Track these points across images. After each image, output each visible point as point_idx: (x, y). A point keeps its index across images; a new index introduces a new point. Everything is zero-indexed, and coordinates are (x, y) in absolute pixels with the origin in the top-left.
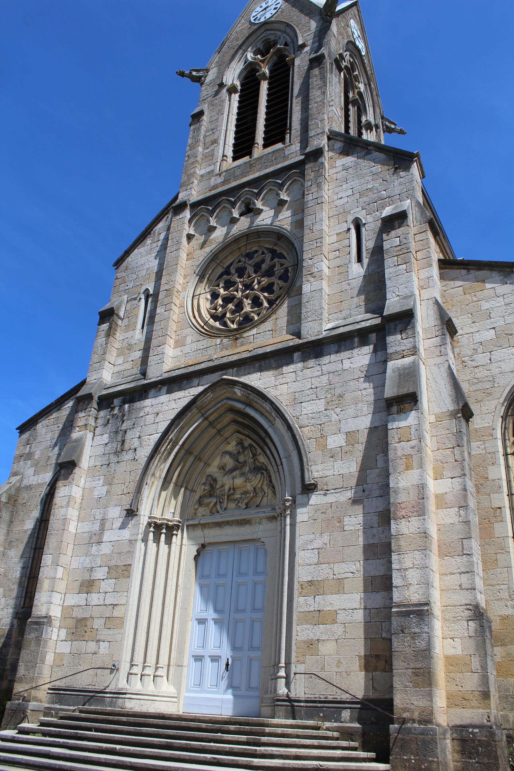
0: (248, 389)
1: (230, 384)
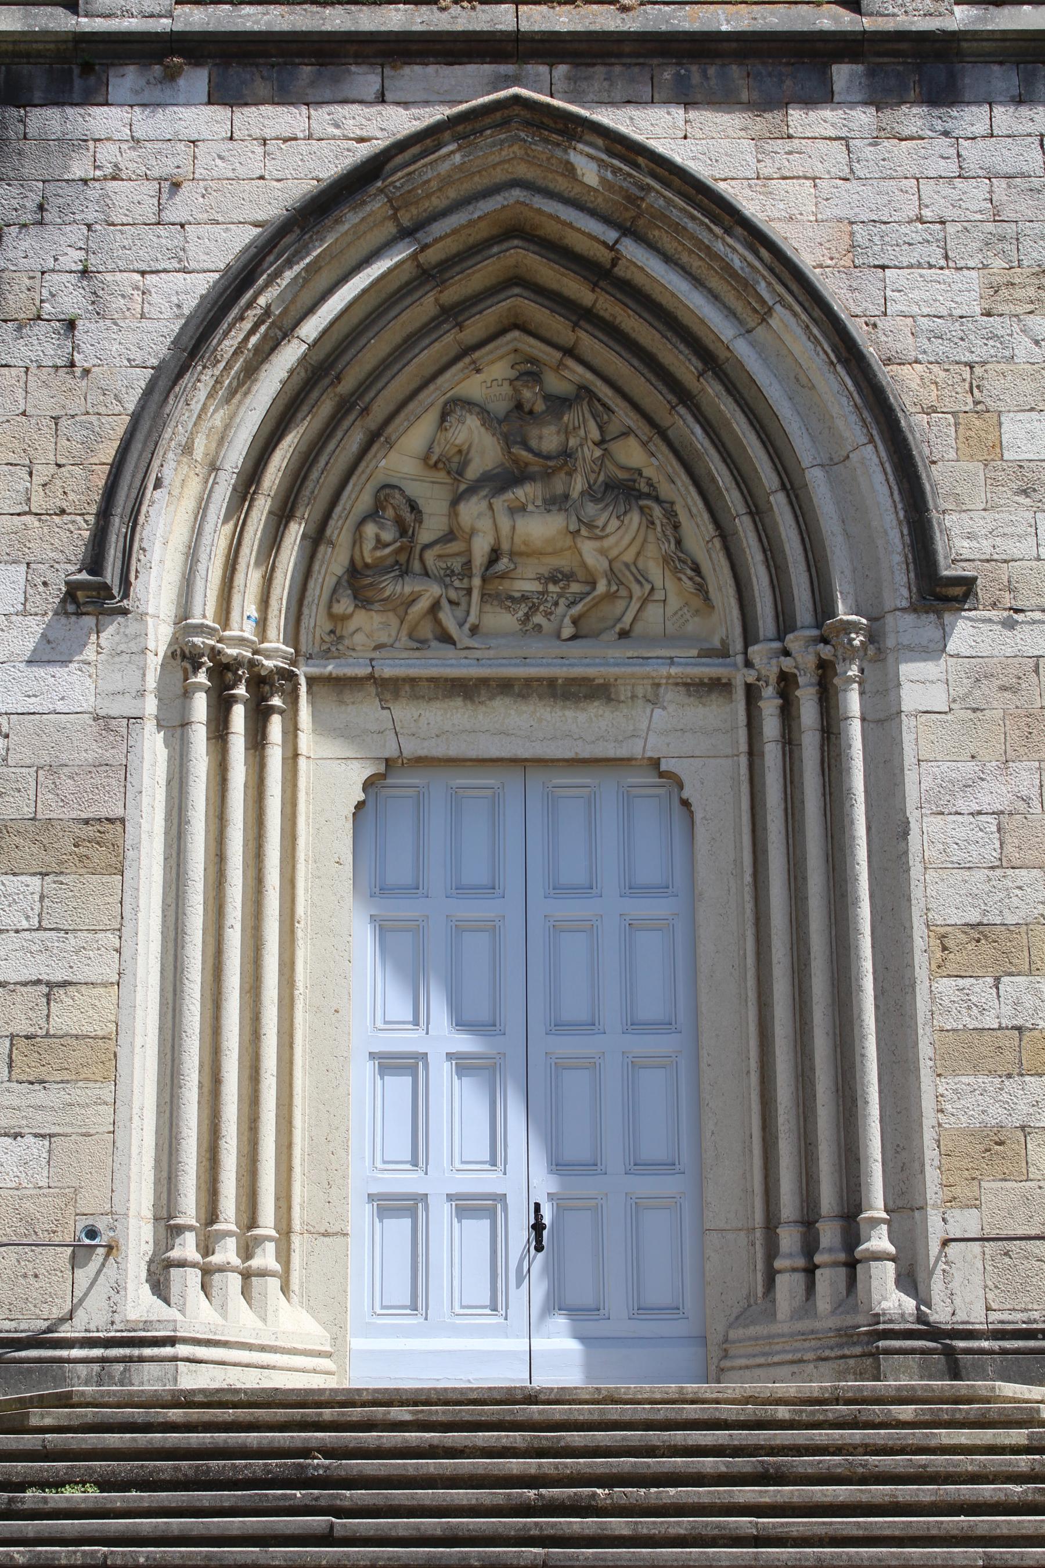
0: (636, 166)
1: (541, 126)
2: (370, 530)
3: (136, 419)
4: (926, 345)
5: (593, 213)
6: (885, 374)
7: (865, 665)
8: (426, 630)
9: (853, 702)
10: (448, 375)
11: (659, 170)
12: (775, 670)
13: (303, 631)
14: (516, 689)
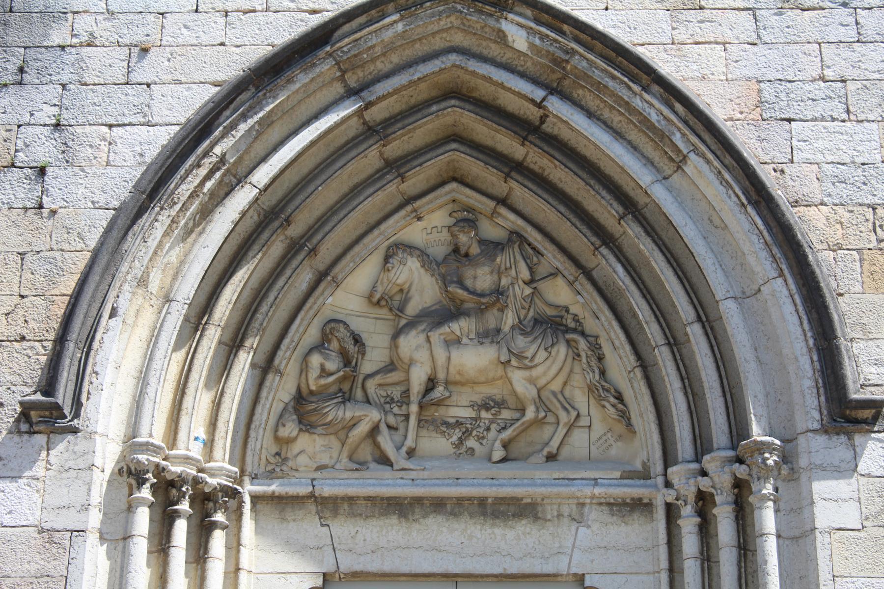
0: (562, 33)
2: (316, 360)
3: (96, 254)
4: (831, 189)
5: (523, 75)
6: (793, 215)
7: (780, 484)
8: (366, 452)
9: (768, 519)
10: (391, 221)
11: (583, 36)
12: (693, 489)
13: (249, 453)
14: (449, 507)
